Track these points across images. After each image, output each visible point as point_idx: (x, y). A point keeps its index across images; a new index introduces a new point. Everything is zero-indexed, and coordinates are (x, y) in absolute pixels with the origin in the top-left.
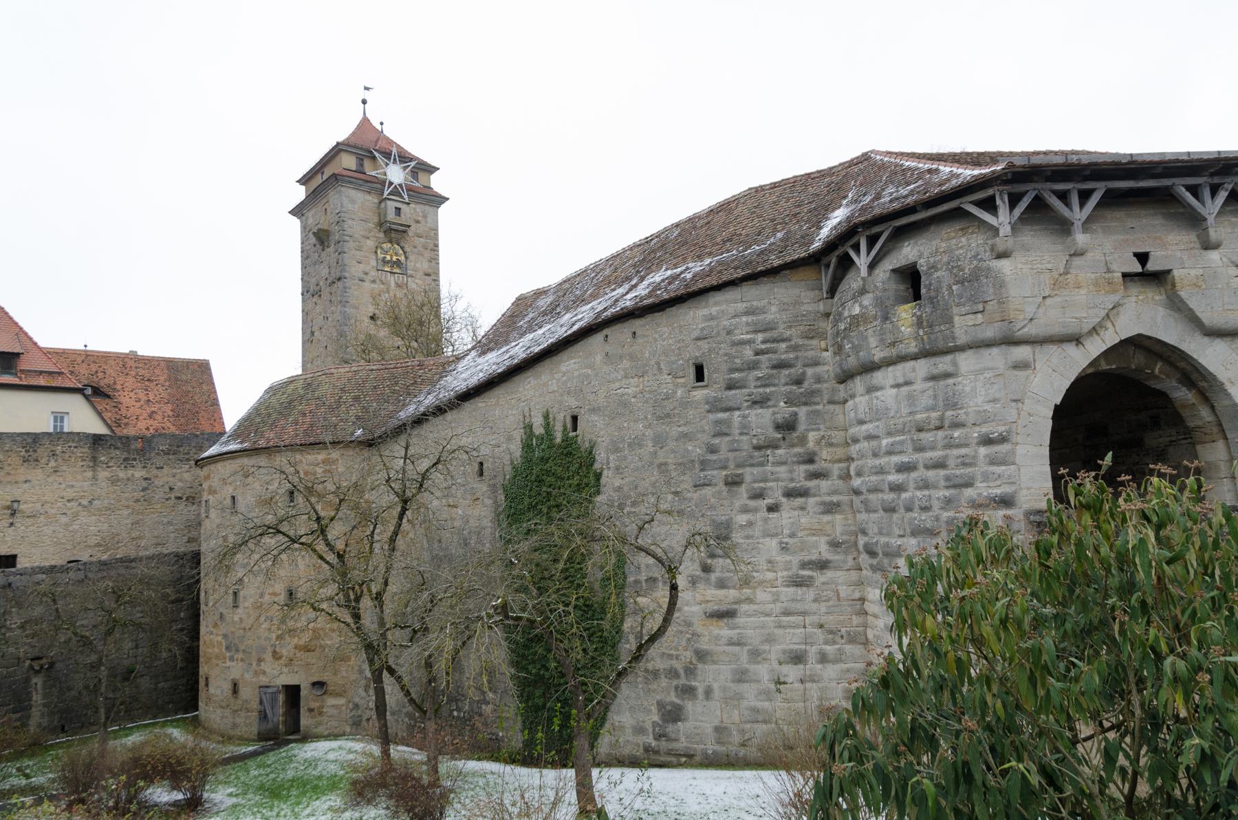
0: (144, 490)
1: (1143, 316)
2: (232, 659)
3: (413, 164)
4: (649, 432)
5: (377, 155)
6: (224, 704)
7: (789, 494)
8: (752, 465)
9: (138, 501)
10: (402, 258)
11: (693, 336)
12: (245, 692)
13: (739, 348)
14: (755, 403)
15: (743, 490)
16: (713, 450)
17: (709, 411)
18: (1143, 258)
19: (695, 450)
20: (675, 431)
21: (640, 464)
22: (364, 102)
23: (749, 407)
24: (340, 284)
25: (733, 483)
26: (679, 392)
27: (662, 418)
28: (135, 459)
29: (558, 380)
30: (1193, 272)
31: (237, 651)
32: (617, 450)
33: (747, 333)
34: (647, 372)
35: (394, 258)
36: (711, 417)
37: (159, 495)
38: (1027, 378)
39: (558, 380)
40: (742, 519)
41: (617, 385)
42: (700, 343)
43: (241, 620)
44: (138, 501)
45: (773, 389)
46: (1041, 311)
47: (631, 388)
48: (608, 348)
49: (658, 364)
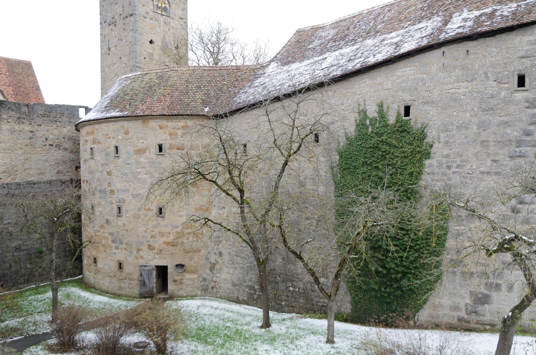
0: (30, 138)
2: (117, 248)
4: (475, 119)
6: (111, 275)
9: (27, 145)
10: (167, 6)
11: (518, 55)
12: (127, 268)
16: (528, 134)
17: (527, 108)
19: (513, 133)
20: (497, 119)
21: (466, 140)
24: (132, 18)
26: (503, 94)
27: (486, 110)
28: (24, 118)
29: (393, 82)
31: (121, 243)
32: (447, 130)
34: (475, 79)
35: (163, 6)
36: (529, 111)
37: (40, 142)
39: (393, 82)
41: (450, 86)
42: (523, 60)
43: (124, 225)
44: (27, 145)
47: (463, 88)
48: (444, 61)
49: (486, 74)
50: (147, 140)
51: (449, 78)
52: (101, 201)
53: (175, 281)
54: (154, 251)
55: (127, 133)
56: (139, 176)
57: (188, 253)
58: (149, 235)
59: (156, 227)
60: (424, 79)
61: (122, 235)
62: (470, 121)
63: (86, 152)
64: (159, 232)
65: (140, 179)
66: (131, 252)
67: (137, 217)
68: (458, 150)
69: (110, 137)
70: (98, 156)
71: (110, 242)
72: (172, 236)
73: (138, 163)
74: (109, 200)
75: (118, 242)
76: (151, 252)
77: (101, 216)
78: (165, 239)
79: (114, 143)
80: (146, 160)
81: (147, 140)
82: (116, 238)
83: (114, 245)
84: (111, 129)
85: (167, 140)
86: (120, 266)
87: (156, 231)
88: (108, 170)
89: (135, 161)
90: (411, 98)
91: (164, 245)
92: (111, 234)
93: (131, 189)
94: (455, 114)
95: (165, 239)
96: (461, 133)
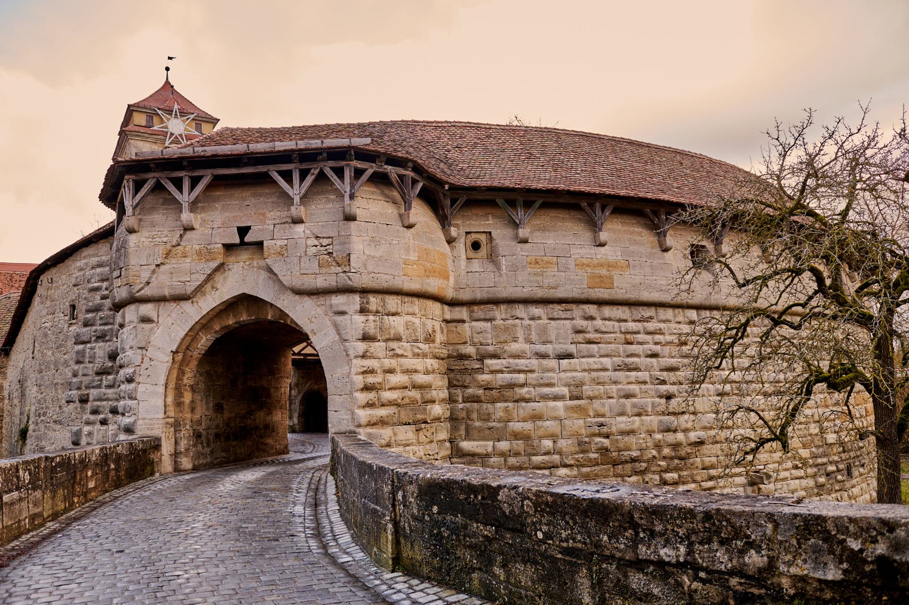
1: (241, 278)
3: (192, 116)
5: (160, 112)
7: (114, 411)
8: (94, 387)
13: (92, 294)
14: (98, 337)
15: (89, 406)
18: (243, 231)
22: (167, 69)
23: (96, 341)
25: (84, 400)
30: (279, 243)
33: (99, 281)
38: (151, 330)
40: (86, 429)
45: (110, 327)
46: (155, 276)
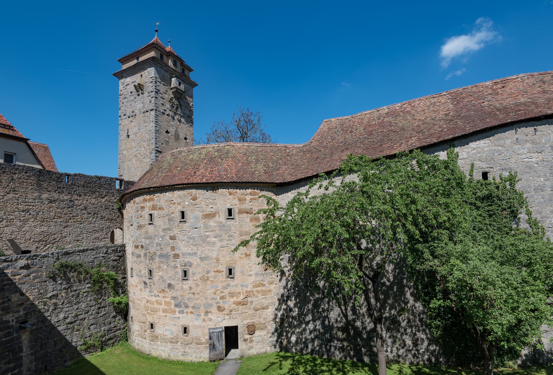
2: (181, 312)
6: (174, 340)
12: (192, 332)
21: (543, 200)
29: (468, 153)
39: (468, 153)
41: (524, 156)
43: (191, 288)
50: (216, 205)
51: (523, 150)
52: (162, 265)
53: (245, 340)
54: (223, 312)
55: (194, 199)
56: (208, 239)
57: (258, 310)
58: (219, 297)
59: (225, 288)
60: (499, 150)
61: (188, 299)
62: (544, 184)
63: (142, 218)
64: (229, 293)
65: (209, 243)
66: (198, 315)
67: (205, 279)
68: (537, 208)
69: (174, 203)
70: (157, 221)
71: (173, 307)
72: (242, 295)
73: (206, 226)
74: (172, 264)
75: (183, 306)
76: (221, 313)
77: (161, 281)
78: (235, 299)
79: (180, 208)
80: (215, 224)
81: (216, 205)
82: (180, 302)
83: (177, 309)
84: (176, 196)
85: (236, 205)
86: (185, 330)
87: (226, 292)
88: (172, 235)
89: (204, 225)
90: (488, 166)
91: (234, 305)
92: (174, 298)
93: (199, 253)
94: (531, 178)
95: (235, 299)
96: (538, 194)
